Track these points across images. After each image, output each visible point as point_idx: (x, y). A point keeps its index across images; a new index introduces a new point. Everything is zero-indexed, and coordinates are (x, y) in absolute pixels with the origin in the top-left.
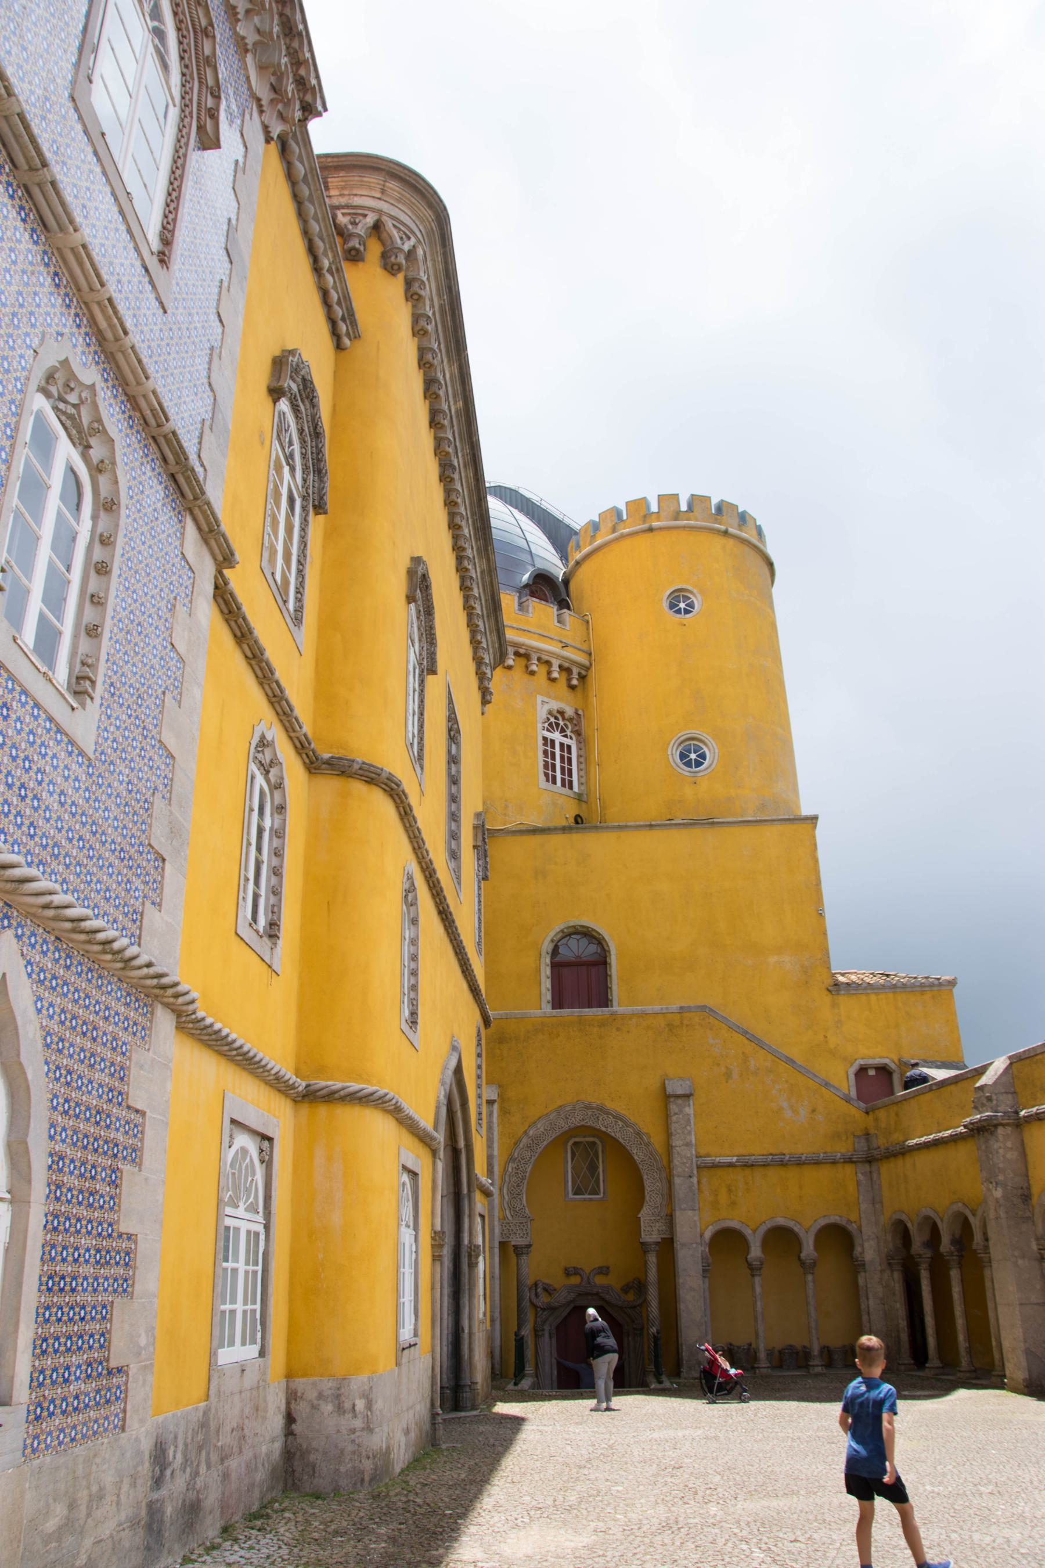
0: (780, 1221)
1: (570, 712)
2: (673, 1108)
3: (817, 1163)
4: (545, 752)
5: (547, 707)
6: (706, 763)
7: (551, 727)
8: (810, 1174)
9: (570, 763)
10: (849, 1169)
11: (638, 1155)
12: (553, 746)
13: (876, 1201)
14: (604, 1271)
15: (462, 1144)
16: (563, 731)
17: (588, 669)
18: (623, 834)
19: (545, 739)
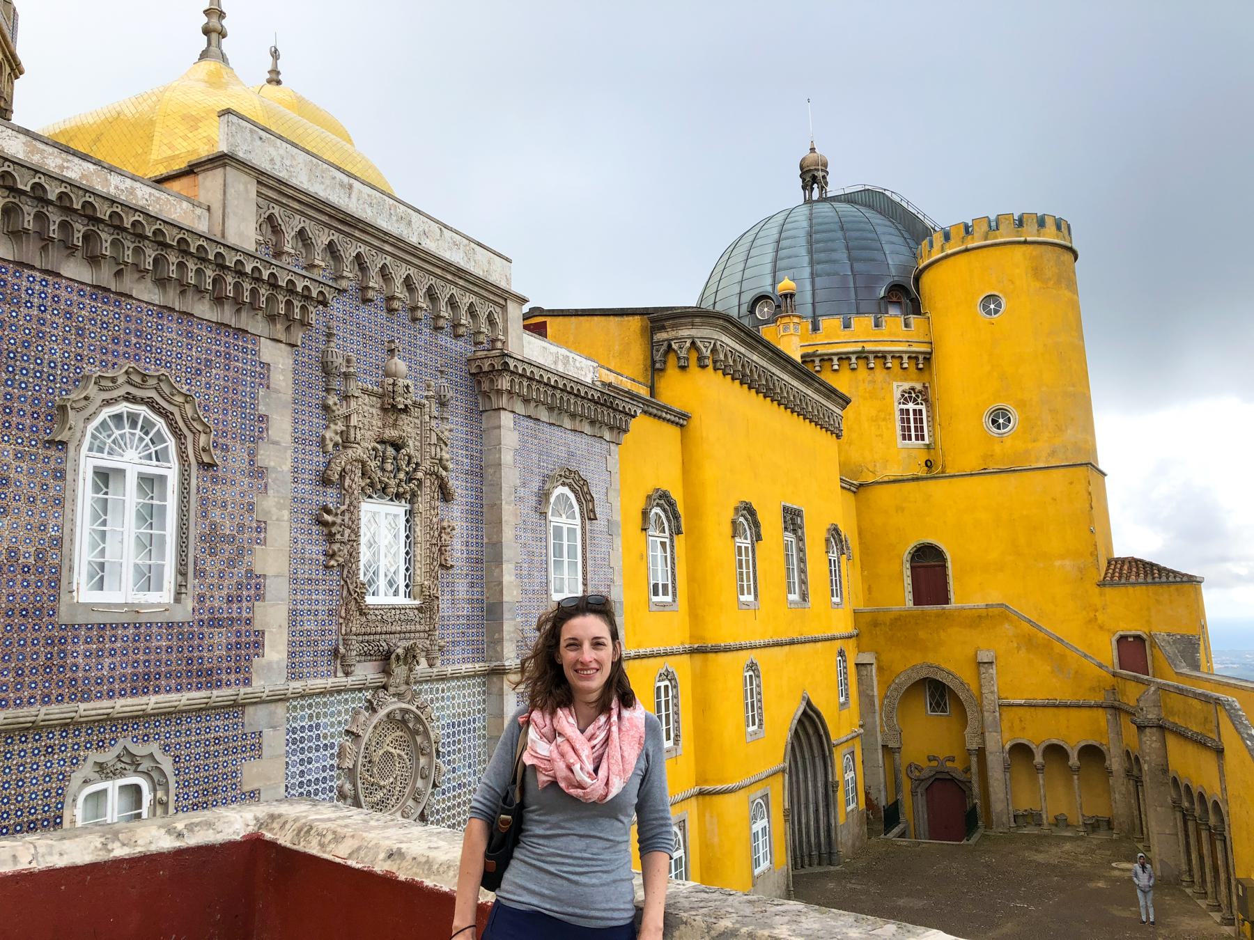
0: (1055, 741)
1: (919, 387)
2: (983, 670)
3: (1079, 707)
4: (902, 420)
5: (901, 389)
6: (1011, 425)
7: (906, 401)
8: (1074, 713)
9: (921, 422)
10: (1100, 710)
11: (962, 696)
12: (908, 414)
13: (1119, 734)
14: (952, 759)
15: (822, 732)
16: (915, 400)
17: (930, 353)
18: (955, 479)
19: (902, 410)
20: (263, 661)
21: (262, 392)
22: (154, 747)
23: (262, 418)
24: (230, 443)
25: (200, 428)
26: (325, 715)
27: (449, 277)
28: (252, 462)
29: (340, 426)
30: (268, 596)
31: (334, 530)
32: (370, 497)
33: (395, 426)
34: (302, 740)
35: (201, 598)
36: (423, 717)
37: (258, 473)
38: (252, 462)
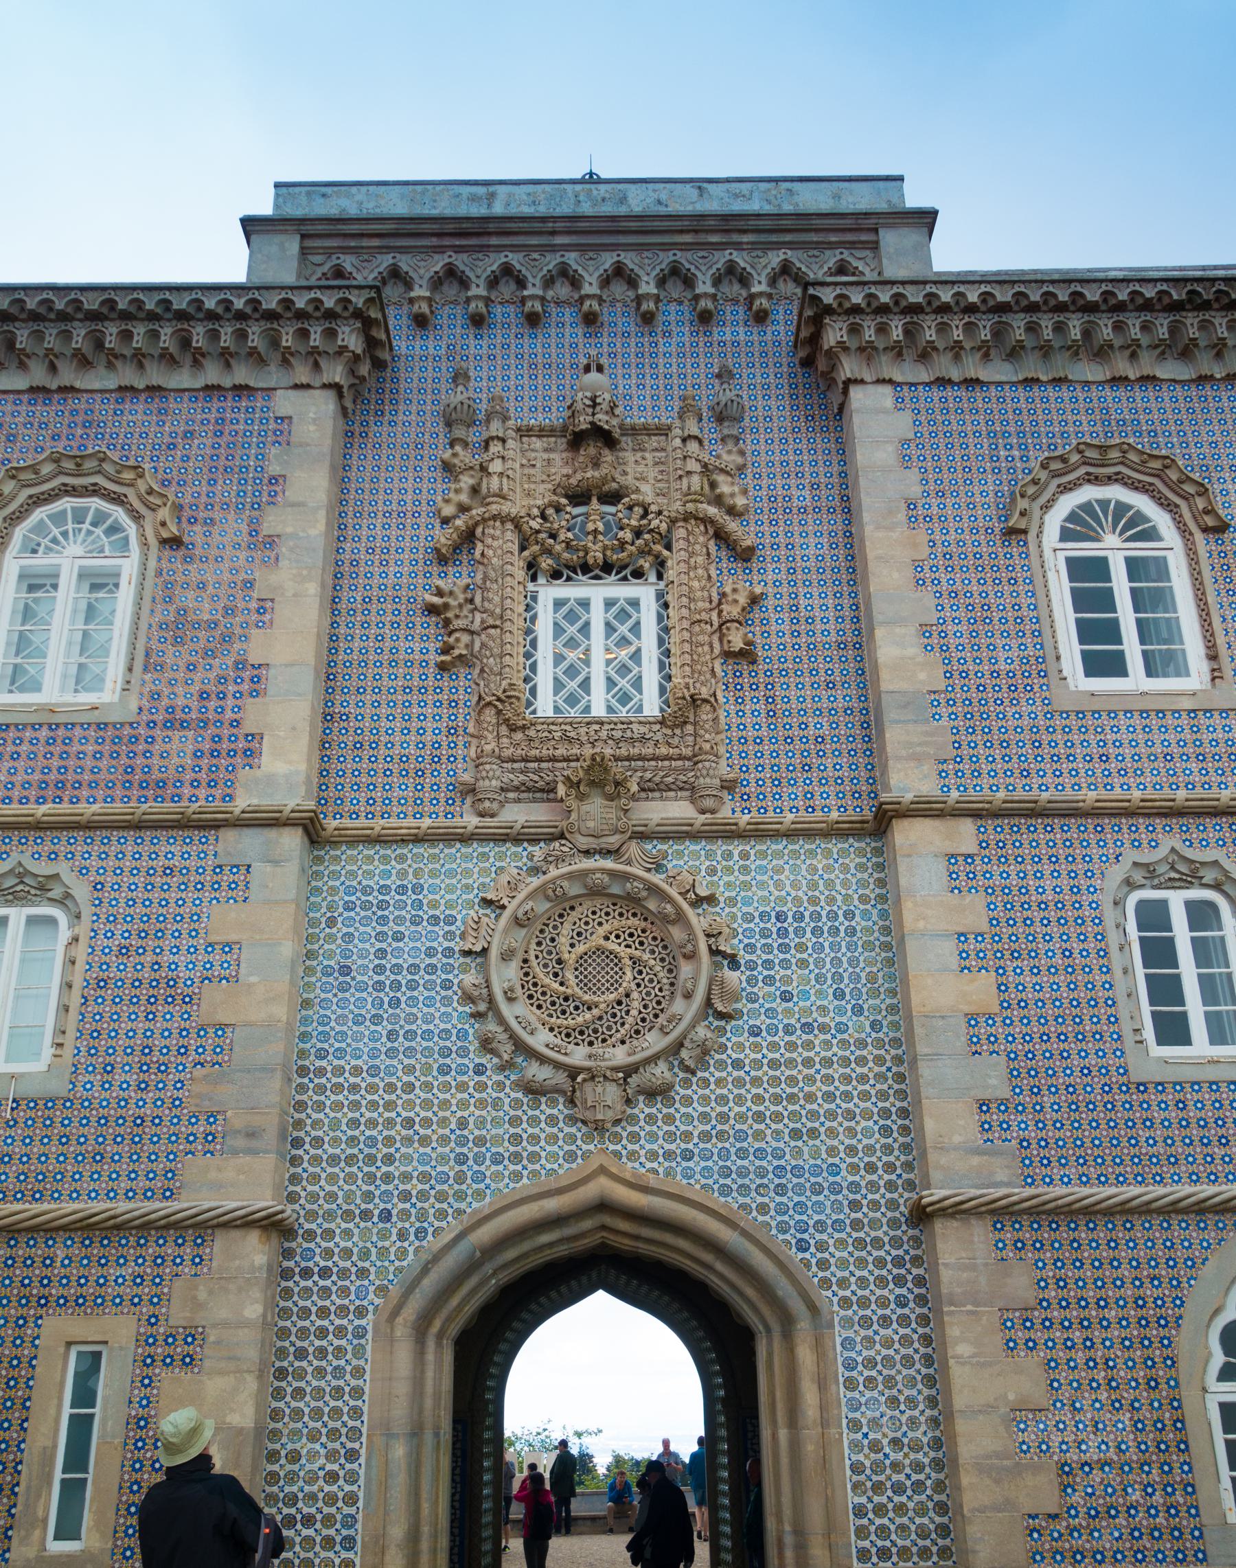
20: (258, 773)
21: (274, 451)
22: (62, 868)
23: (274, 480)
24: (217, 515)
25: (159, 502)
26: (433, 874)
27: (714, 238)
28: (254, 532)
29: (467, 481)
30: (271, 690)
31: (450, 615)
32: (569, 579)
33: (596, 465)
34: (383, 905)
35: (155, 696)
36: (673, 892)
37: (265, 545)
38: (254, 532)
